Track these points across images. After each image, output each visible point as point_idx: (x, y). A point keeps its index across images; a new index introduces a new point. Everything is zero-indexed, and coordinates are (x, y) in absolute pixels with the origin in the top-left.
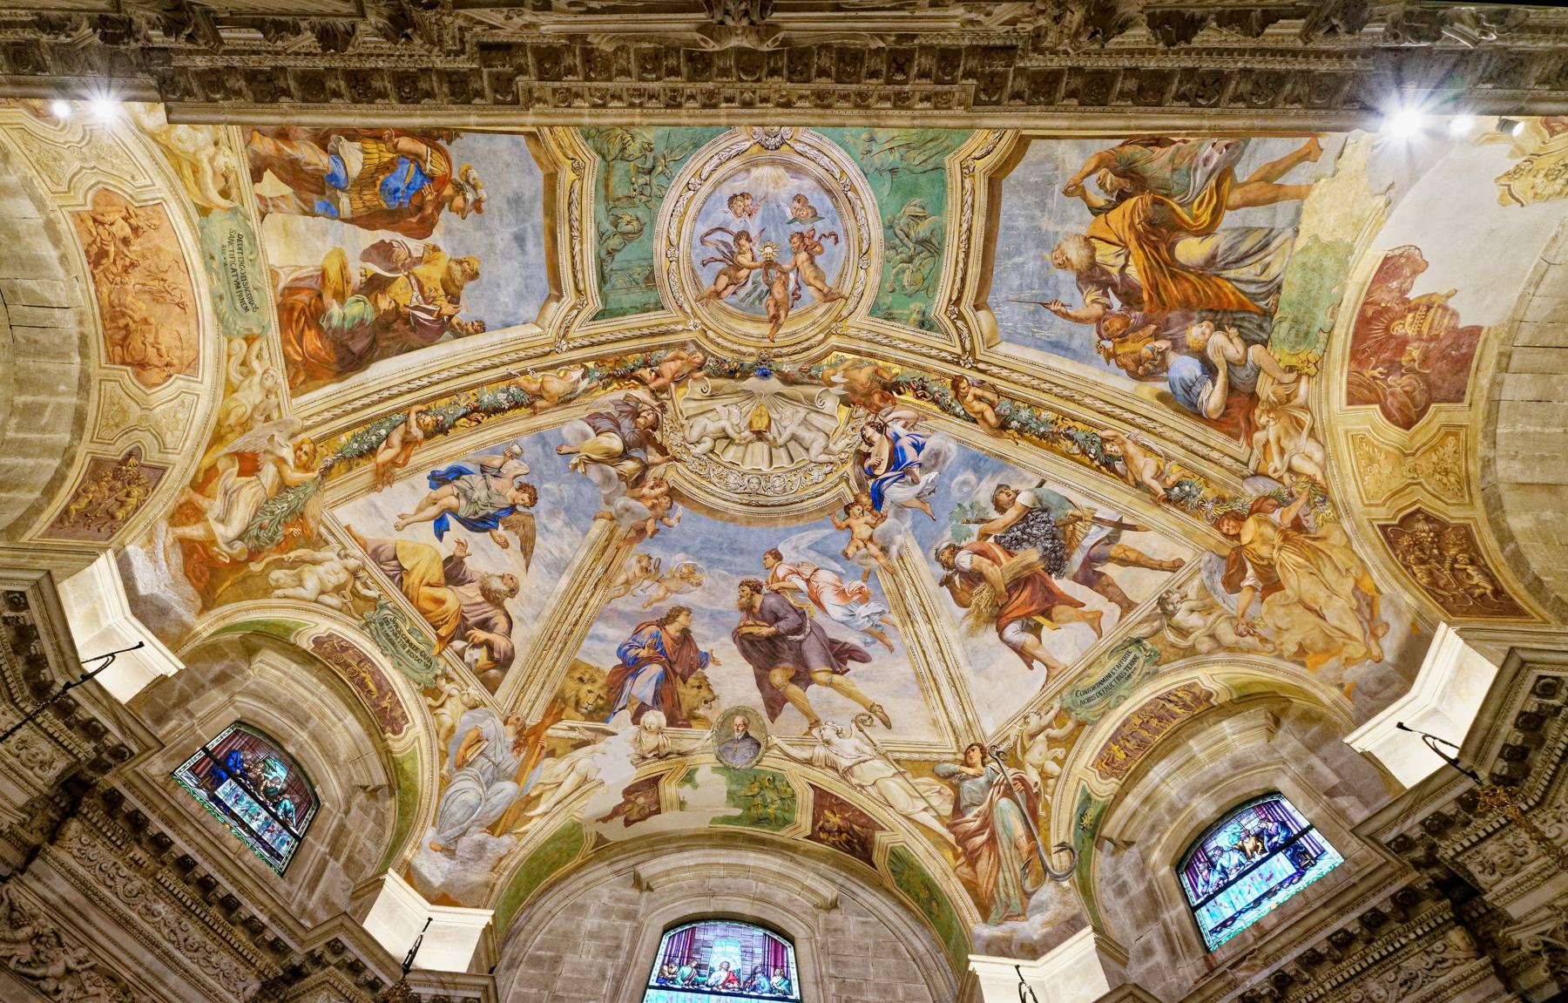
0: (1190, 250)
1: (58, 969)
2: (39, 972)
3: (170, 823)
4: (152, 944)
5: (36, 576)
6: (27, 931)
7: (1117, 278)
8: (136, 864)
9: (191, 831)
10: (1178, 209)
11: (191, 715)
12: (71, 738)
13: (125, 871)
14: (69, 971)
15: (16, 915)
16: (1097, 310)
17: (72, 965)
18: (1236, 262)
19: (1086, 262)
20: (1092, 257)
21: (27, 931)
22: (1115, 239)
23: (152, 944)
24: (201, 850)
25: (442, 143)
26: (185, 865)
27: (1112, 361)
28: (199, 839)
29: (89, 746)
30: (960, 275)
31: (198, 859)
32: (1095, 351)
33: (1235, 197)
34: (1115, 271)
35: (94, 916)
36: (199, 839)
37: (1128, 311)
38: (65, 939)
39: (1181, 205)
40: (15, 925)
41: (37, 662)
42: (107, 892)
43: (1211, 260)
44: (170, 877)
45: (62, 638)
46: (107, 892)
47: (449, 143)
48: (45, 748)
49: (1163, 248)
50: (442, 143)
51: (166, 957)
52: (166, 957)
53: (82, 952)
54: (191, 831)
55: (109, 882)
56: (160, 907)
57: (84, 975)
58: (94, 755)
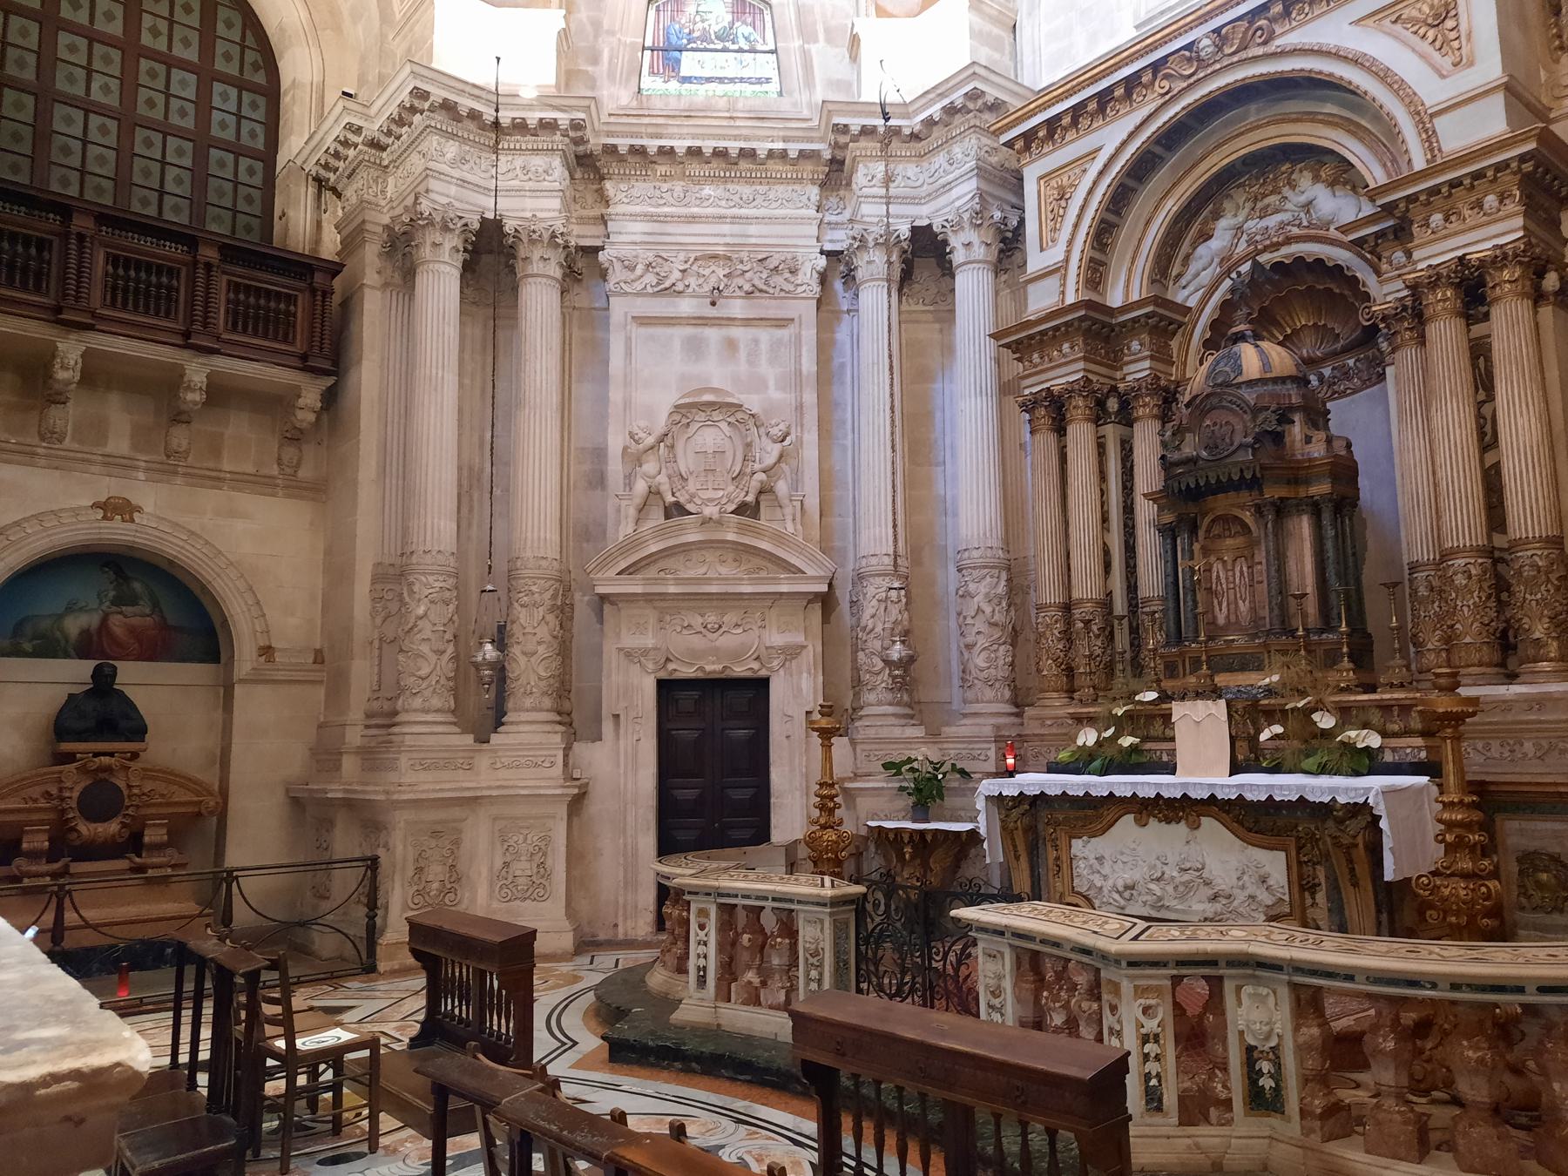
1: (677, 275)
2: (667, 284)
3: (659, 136)
4: (721, 219)
5: (408, 68)
6: (640, 269)
8: (665, 178)
9: (675, 130)
11: (611, 33)
12: (544, 141)
13: (665, 186)
14: (683, 271)
15: (626, 263)
17: (682, 268)
21: (640, 269)
23: (721, 219)
24: (694, 137)
26: (695, 152)
28: (685, 131)
29: (558, 137)
31: (697, 143)
35: (669, 228)
36: (685, 131)
38: (664, 255)
40: (632, 269)
41: (474, 115)
42: (666, 209)
44: (695, 168)
45: (468, 89)
46: (666, 209)
48: (538, 162)
51: (736, 219)
52: (736, 219)
53: (682, 256)
54: (675, 130)
55: (663, 202)
56: (708, 190)
57: (695, 267)
58: (567, 140)
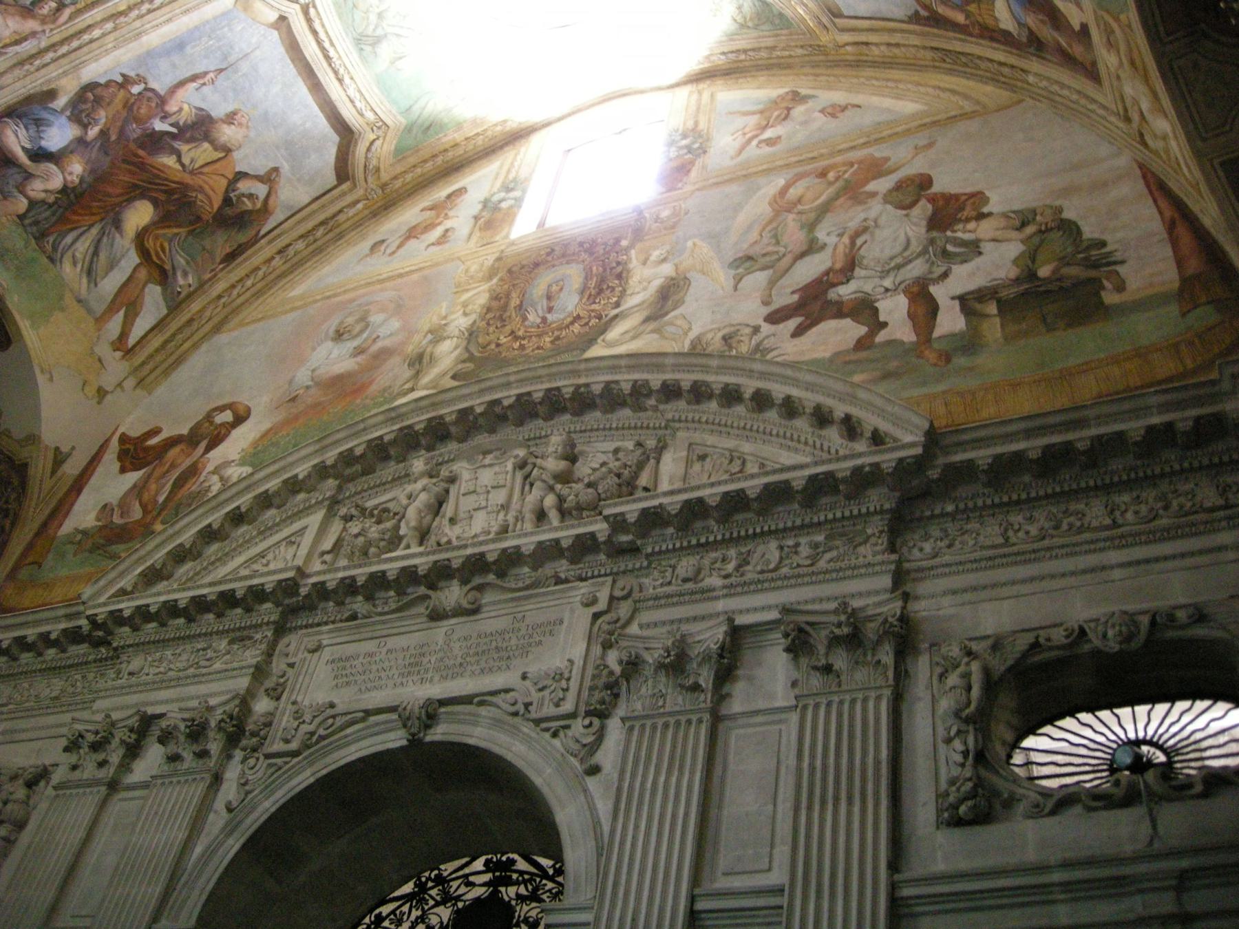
0: (140, 215)
7: (177, 145)
10: (175, 230)
16: (172, 107)
18: (99, 241)
19: (215, 134)
20: (212, 142)
22: (206, 170)
25: (923, 13)
27: (120, 79)
30: (322, 35)
32: (141, 72)
33: (143, 274)
34: (184, 148)
37: (145, 130)
39: (177, 234)
43: (117, 224)
47: (917, 12)
49: (162, 197)
50: (923, 13)
